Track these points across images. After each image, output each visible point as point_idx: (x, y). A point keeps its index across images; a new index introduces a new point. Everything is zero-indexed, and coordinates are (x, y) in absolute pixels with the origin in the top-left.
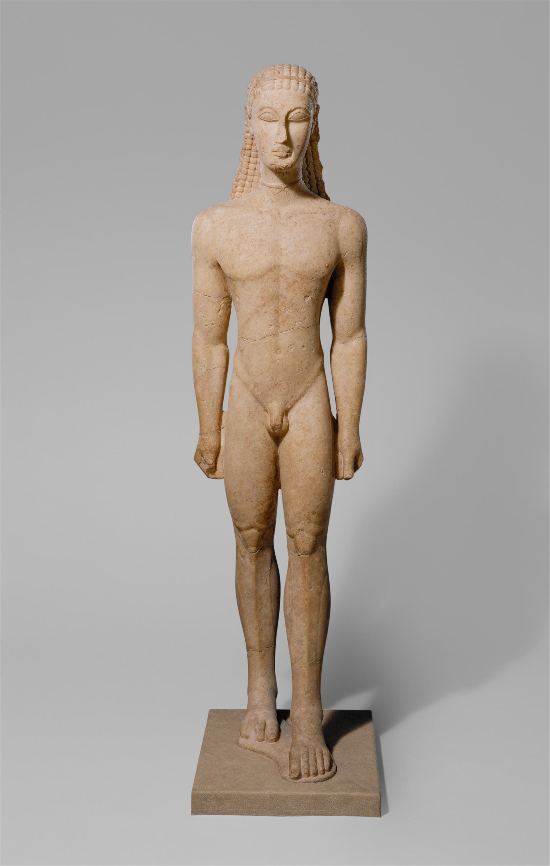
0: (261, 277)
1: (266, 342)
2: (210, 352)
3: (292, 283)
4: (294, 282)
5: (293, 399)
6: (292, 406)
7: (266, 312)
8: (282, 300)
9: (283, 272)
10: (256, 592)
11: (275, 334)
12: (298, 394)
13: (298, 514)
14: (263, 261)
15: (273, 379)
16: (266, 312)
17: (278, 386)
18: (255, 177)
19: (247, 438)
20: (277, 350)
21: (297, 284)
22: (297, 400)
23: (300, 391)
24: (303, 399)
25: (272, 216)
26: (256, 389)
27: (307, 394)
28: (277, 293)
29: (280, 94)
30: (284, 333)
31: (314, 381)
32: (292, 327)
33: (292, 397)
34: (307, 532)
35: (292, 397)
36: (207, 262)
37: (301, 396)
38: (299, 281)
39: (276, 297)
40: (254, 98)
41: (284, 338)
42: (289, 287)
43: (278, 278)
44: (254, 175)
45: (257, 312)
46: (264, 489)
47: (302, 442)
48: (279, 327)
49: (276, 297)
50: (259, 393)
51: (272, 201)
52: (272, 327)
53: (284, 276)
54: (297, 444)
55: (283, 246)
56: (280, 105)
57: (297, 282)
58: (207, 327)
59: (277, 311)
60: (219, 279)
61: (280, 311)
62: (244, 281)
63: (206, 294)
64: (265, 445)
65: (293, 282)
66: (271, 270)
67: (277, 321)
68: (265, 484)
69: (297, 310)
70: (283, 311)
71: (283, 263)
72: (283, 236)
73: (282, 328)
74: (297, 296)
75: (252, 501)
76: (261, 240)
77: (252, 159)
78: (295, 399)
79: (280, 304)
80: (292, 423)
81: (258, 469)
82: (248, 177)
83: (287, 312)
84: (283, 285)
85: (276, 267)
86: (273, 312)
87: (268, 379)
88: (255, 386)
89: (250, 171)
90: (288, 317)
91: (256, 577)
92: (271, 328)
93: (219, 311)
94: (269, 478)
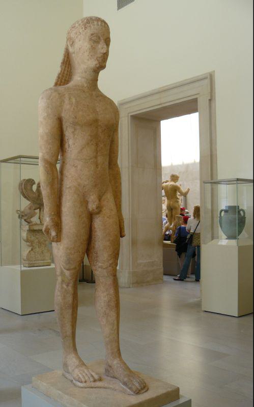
0: (91, 125)
9: (99, 124)
10: (73, 304)
11: (96, 157)
15: (95, 182)
16: (92, 144)
36: (56, 116)
42: (102, 132)
45: (88, 144)
54: (108, 217)
59: (97, 144)
76: (88, 106)
84: (100, 130)
85: (96, 121)
88: (84, 186)
89: (65, 75)
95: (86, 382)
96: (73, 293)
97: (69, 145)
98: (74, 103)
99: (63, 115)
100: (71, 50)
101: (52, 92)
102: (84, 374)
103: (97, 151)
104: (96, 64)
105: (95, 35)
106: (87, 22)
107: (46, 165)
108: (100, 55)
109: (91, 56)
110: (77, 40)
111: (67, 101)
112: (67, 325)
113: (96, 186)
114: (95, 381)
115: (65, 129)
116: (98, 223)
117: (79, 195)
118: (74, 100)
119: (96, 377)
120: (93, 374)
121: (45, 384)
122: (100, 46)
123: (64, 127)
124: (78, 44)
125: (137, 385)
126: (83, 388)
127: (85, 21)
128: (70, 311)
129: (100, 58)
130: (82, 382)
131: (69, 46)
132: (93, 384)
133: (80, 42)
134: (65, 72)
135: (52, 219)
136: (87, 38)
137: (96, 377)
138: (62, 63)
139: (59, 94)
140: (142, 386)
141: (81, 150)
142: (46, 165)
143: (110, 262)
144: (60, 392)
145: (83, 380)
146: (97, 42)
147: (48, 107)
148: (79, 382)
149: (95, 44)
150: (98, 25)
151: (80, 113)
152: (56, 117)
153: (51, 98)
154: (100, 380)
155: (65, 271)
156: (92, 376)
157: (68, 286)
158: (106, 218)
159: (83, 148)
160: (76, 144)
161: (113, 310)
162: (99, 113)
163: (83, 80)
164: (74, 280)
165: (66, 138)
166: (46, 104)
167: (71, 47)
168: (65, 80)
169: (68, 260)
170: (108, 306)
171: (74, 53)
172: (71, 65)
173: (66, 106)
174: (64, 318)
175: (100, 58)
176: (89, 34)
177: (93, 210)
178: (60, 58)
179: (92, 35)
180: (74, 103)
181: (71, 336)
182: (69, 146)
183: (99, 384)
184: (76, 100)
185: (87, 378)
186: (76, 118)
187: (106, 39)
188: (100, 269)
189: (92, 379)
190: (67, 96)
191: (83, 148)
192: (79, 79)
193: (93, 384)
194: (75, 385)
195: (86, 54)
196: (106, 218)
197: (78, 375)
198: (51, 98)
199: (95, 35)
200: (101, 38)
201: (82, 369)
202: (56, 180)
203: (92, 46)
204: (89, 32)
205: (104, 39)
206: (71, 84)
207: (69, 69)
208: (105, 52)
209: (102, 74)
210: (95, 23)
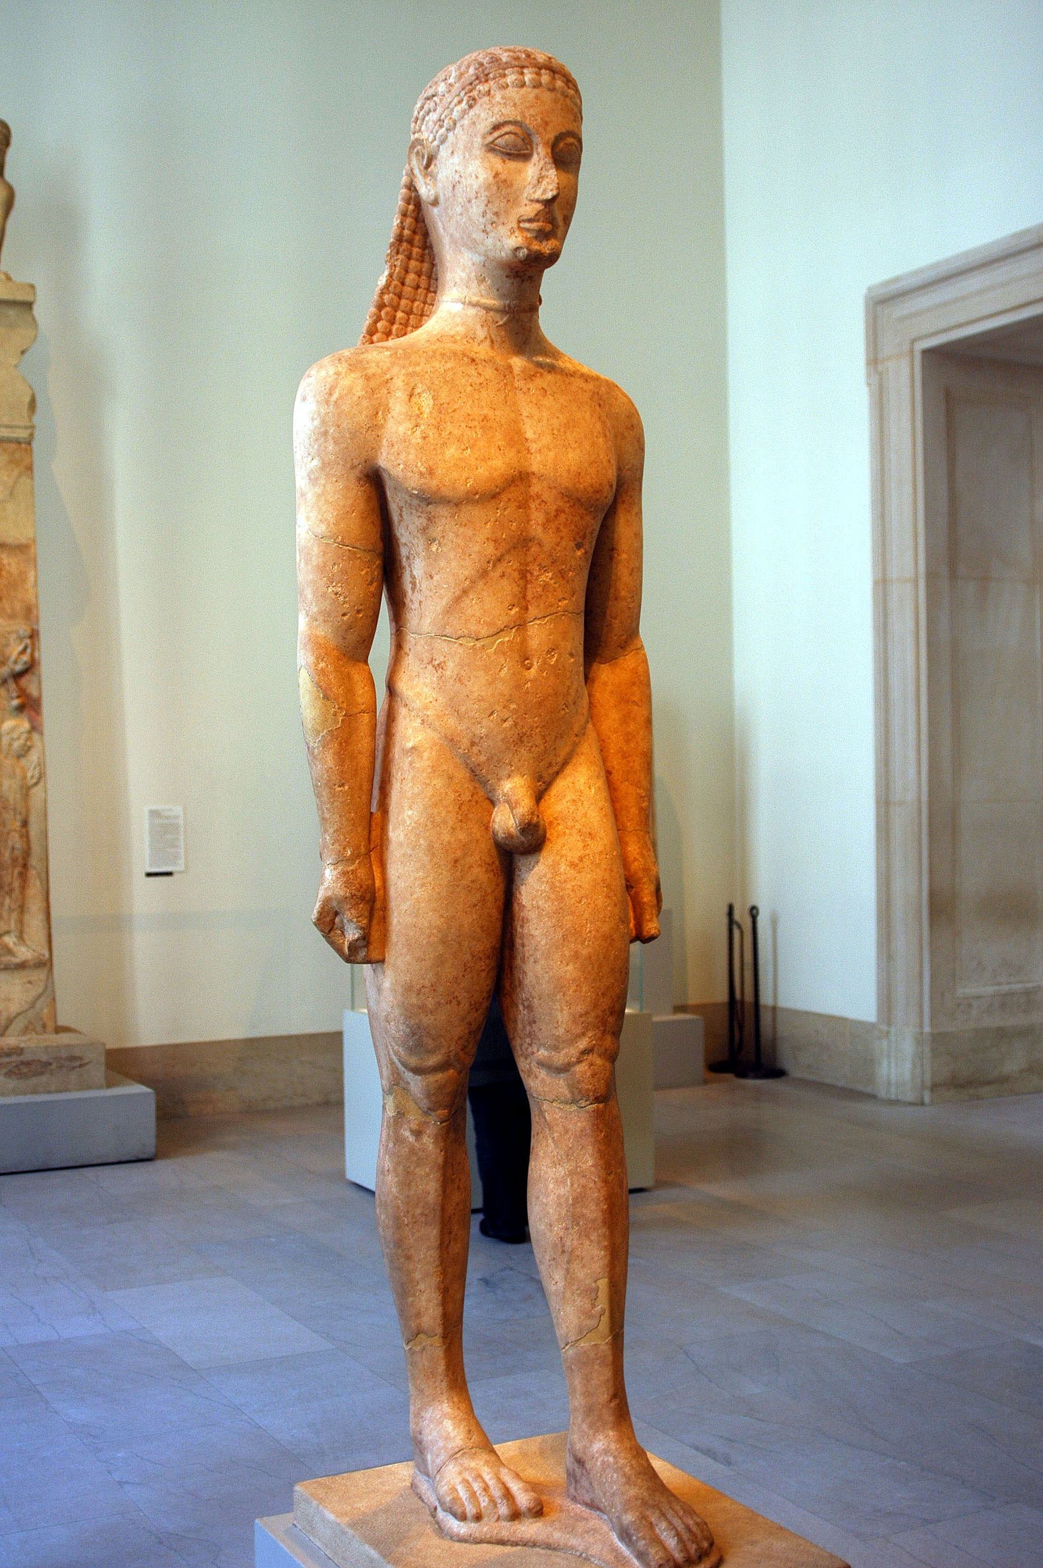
0: (494, 496)
1: (502, 643)
2: (349, 676)
3: (553, 513)
4: (559, 511)
5: (551, 771)
6: (549, 785)
7: (503, 576)
8: (534, 549)
9: (536, 488)
10: (443, 1209)
11: (521, 625)
12: (560, 760)
13: (581, 1016)
14: (497, 464)
15: (516, 724)
16: (503, 576)
17: (525, 739)
18: (416, 303)
19: (456, 861)
20: (524, 659)
21: (563, 517)
22: (557, 773)
23: (563, 753)
24: (568, 770)
25: (496, 369)
26: (475, 749)
27: (574, 760)
28: (524, 534)
29: (537, 97)
30: (538, 622)
31: (582, 733)
32: (553, 610)
33: (550, 765)
34: (600, 1056)
35: (550, 765)
36: (353, 467)
37: (565, 764)
38: (567, 509)
39: (522, 543)
40: (471, 107)
41: (538, 635)
42: (548, 521)
43: (527, 501)
44: (413, 301)
45: (484, 574)
46: (484, 974)
47: (581, 859)
48: (527, 609)
49: (522, 543)
50: (482, 758)
51: (492, 342)
52: (516, 610)
53: (538, 496)
54: (573, 865)
55: (529, 434)
56: (539, 120)
57: (564, 512)
58: (345, 618)
59: (524, 575)
60: (373, 510)
61: (528, 575)
62: (456, 505)
63: (347, 542)
64: (491, 875)
65: (557, 511)
66: (513, 481)
67: (524, 597)
68: (487, 961)
69: (562, 574)
70: (536, 573)
71: (534, 468)
72: (525, 414)
73: (533, 611)
74: (564, 543)
75: (459, 1003)
76: (485, 418)
77: (413, 264)
78: (555, 769)
79: (530, 559)
80: (551, 823)
81: (478, 930)
82: (403, 302)
83: (543, 578)
84: (537, 517)
85: (520, 478)
86: (516, 575)
87: (506, 725)
88: (473, 744)
89: (407, 290)
90: (545, 587)
91: (444, 1175)
92: (513, 612)
93: (371, 583)
94: (493, 948)
95: (478, 1518)
96: (440, 1160)
97: (413, 577)
98: (427, 410)
99: (384, 461)
100: (425, 191)
101: (338, 374)
102: (476, 1486)
103: (522, 602)
104: (517, 249)
105: (507, 129)
106: (477, 78)
107: (322, 665)
108: (530, 210)
109: (496, 214)
110: (444, 153)
111: (398, 406)
112: (422, 1286)
113: (520, 739)
114: (515, 1515)
115: (395, 518)
116: (535, 884)
117: (451, 778)
118: (426, 402)
119: (524, 1499)
120: (515, 1487)
121: (331, 1517)
122: (531, 170)
123: (393, 507)
124: (448, 166)
125: (671, 1542)
126: (466, 1541)
127: (472, 71)
128: (433, 1233)
129: (530, 221)
130: (463, 1517)
131: (417, 172)
132: (506, 1529)
133: (456, 159)
134: (408, 281)
135: (344, 873)
136: (478, 141)
137: (524, 1499)
138: (392, 245)
139: (368, 378)
140: (693, 1548)
141: (457, 600)
142: (322, 665)
143: (583, 1044)
144: (374, 1553)
145: (470, 1510)
146: (519, 153)
147: (325, 433)
148: (455, 1515)
149: (513, 165)
150: (523, 85)
151: (452, 452)
152: (356, 472)
153: (336, 396)
154: (538, 1512)
155: (409, 1076)
156: (508, 1495)
157: (418, 1133)
158: (563, 868)
159: (465, 592)
160: (436, 578)
161: (594, 1237)
162: (534, 447)
163: (472, 311)
164: (443, 1112)
165: (404, 551)
166: (316, 423)
167: (425, 176)
168: (409, 313)
169: (414, 1034)
170: (575, 1219)
171: (435, 203)
172: (431, 247)
173: (397, 426)
174: (409, 1258)
175: (530, 221)
176: (484, 126)
177: (510, 836)
178: (391, 223)
179: (496, 127)
180: (427, 410)
181: (439, 1330)
182: (414, 584)
183: (529, 1529)
184: (434, 399)
185: (484, 1502)
186: (431, 472)
187: (559, 138)
188: (543, 1074)
189: (504, 1510)
190: (398, 383)
191: (465, 592)
192: (458, 307)
193: (506, 1529)
194: (440, 1530)
195: (476, 209)
196: (563, 868)
197: (454, 1489)
198: (336, 396)
199: (507, 129)
200: (536, 139)
201: (473, 1464)
202: (366, 718)
203: (496, 175)
204: (485, 116)
205: (546, 144)
206: (418, 336)
207: (426, 266)
208: (549, 195)
209: (550, 279)
210: (511, 78)
